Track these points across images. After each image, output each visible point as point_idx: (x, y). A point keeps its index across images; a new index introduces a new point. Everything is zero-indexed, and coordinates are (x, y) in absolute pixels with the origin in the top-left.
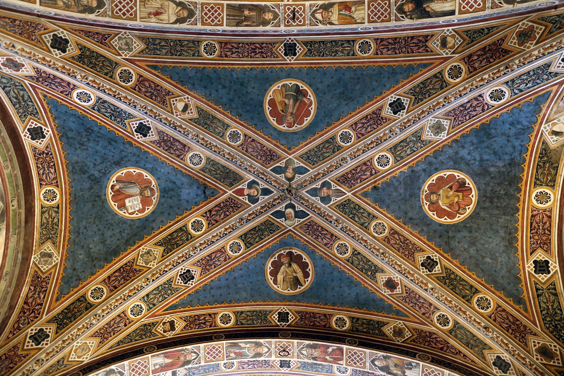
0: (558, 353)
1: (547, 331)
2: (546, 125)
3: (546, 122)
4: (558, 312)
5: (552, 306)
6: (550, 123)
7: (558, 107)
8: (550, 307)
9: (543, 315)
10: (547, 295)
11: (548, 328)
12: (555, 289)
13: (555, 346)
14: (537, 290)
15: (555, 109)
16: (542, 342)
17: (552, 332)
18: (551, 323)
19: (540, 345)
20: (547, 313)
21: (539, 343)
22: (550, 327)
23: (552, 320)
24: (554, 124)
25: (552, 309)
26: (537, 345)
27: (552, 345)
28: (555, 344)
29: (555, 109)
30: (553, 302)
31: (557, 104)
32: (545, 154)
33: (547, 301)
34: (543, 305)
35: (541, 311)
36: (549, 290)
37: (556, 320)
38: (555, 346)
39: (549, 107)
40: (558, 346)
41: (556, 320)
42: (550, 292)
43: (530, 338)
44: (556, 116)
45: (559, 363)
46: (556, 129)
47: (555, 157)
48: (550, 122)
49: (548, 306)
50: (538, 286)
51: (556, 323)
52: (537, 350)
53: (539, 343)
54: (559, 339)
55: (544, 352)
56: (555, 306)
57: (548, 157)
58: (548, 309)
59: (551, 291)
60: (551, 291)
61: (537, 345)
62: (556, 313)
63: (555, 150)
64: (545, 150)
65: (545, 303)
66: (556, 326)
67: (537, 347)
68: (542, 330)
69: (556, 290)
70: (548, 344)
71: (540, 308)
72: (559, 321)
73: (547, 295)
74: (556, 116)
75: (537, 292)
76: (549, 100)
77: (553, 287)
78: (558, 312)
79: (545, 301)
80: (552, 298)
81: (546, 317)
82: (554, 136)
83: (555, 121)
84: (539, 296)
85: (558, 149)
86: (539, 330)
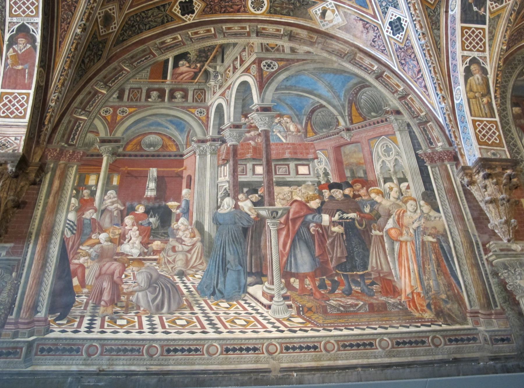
0: (111, 31)
1: (127, 19)
2: (333, 5)
3: (336, 5)
4: (148, 27)
5: (151, 21)
6: (335, 8)
7: (350, 14)
8: (150, 19)
9: (141, 14)
10: (160, 15)
11: (129, 19)
12: (168, 21)
13: (115, 27)
14: (164, 6)
15: (349, 12)
16: (115, 16)
17: (127, 23)
18: (135, 22)
19: (112, 14)
20: (143, 18)
21: (114, 13)
22: (131, 21)
23: (138, 22)
24: (333, 11)
25: (149, 21)
26: (112, 12)
27: (116, 25)
28: (117, 28)
29: (349, 12)
30: (155, 22)
31: (353, 13)
32: (303, 5)
33: (155, 16)
34: (150, 13)
35: (144, 12)
36: (166, 16)
37: (139, 26)
38: (115, 27)
39: (351, 6)
40: (116, 30)
41: (139, 26)
42: (164, 18)
43: (116, 4)
44: (341, 13)
45: (102, 32)
46: (328, 13)
47: (300, 13)
48: (336, 8)
49: (150, 17)
50: (167, 6)
51: (137, 26)
52: (106, 12)
53: (114, 13)
54: (122, 30)
55: (108, 19)
56: (152, 23)
57: (300, 6)
58: (147, 18)
59: (166, 18)
60: (166, 18)
61: (112, 12)
62: (146, 25)
63: (307, 12)
64: (306, 4)
65: (153, 14)
66: (133, 26)
67: (110, 12)
68: (126, 14)
69: (167, 22)
70: (116, 21)
71: (146, 11)
72: (139, 28)
73: (160, 15)
74: (341, 13)
75: (162, 6)
76: (359, 7)
77: (170, 20)
78: (148, 27)
79: (155, 14)
80: (159, 20)
81: (140, 17)
82: (321, 11)
83: (336, 12)
84: (158, 8)
85: (307, 15)
86: (126, 12)
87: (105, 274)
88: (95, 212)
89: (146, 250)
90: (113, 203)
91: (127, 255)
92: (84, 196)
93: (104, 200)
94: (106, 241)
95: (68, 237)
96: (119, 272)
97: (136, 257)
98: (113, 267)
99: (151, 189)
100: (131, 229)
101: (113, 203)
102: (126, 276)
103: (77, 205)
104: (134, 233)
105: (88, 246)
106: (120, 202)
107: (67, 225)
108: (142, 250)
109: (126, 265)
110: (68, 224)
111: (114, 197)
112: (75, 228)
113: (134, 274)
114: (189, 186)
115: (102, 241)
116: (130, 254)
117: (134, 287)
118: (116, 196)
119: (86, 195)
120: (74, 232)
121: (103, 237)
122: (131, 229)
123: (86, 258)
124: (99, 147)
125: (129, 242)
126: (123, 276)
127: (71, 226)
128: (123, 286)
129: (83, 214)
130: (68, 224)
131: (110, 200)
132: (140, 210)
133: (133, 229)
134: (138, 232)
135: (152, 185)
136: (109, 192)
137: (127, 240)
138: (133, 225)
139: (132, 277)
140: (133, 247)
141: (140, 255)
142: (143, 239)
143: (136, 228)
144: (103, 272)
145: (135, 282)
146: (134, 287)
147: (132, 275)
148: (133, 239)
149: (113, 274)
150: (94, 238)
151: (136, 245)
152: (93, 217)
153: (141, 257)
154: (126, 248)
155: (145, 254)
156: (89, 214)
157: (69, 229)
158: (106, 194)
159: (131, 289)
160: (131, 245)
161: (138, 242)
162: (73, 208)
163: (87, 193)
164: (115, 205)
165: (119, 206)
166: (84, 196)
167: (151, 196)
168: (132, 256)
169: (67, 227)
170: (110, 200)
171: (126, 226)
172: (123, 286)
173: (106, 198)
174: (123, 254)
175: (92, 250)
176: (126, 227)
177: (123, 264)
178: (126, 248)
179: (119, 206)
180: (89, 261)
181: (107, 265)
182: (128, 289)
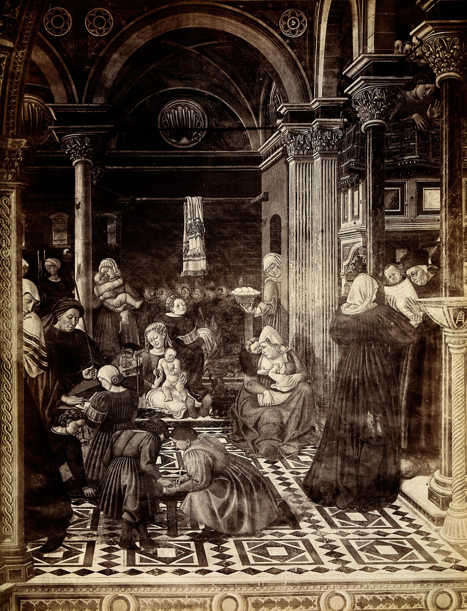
87: (122, 455)
88: (81, 315)
89: (198, 404)
90: (115, 292)
91: (162, 415)
92: (50, 275)
93: (95, 284)
94: (113, 384)
95: (34, 376)
96: (150, 452)
97: (178, 418)
98: (135, 441)
99: (195, 256)
100: (163, 356)
101: (115, 292)
102: (165, 460)
103: (37, 298)
104: (170, 366)
105: (77, 395)
106: (128, 289)
107: (25, 348)
108: (190, 404)
109: (162, 436)
110: (28, 345)
111: (116, 278)
112: (44, 354)
113: (179, 455)
114: (276, 247)
115: (106, 385)
116: (166, 412)
117: (182, 482)
118: (118, 273)
119: (52, 270)
120: (45, 364)
121: (106, 373)
122: (163, 356)
123: (79, 422)
124: (60, 136)
125: (160, 385)
126: (159, 461)
127: (35, 350)
128: (160, 481)
129: (56, 321)
130: (28, 345)
131: (108, 285)
132: (175, 309)
133: (167, 356)
134: (176, 363)
135: (194, 244)
136: (104, 262)
137: (157, 381)
138: (166, 347)
139: (176, 462)
140: (172, 398)
141: (185, 416)
142: (189, 378)
143: (171, 352)
144: (117, 452)
145: (183, 473)
146: (182, 482)
147: (175, 457)
148: (170, 378)
149: (137, 456)
150: (89, 377)
151: (176, 393)
152: (78, 327)
153: (190, 419)
154: (156, 399)
155: (197, 411)
156: (67, 321)
157: (32, 357)
158: (96, 269)
159: (176, 488)
160: (167, 392)
161: (179, 386)
162: (31, 305)
163: (54, 266)
164: (121, 297)
165: (130, 300)
166: (50, 275)
167: (195, 272)
168: (171, 416)
169: (26, 352)
170: (108, 285)
171: (151, 347)
172: (160, 481)
173: (97, 278)
174: (151, 412)
175: (87, 404)
176: (151, 351)
177: (156, 435)
178: (156, 399)
179: (130, 300)
180: (86, 428)
181: (124, 436)
182: (170, 486)
